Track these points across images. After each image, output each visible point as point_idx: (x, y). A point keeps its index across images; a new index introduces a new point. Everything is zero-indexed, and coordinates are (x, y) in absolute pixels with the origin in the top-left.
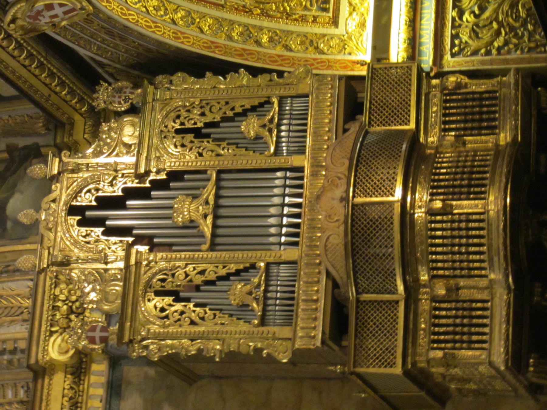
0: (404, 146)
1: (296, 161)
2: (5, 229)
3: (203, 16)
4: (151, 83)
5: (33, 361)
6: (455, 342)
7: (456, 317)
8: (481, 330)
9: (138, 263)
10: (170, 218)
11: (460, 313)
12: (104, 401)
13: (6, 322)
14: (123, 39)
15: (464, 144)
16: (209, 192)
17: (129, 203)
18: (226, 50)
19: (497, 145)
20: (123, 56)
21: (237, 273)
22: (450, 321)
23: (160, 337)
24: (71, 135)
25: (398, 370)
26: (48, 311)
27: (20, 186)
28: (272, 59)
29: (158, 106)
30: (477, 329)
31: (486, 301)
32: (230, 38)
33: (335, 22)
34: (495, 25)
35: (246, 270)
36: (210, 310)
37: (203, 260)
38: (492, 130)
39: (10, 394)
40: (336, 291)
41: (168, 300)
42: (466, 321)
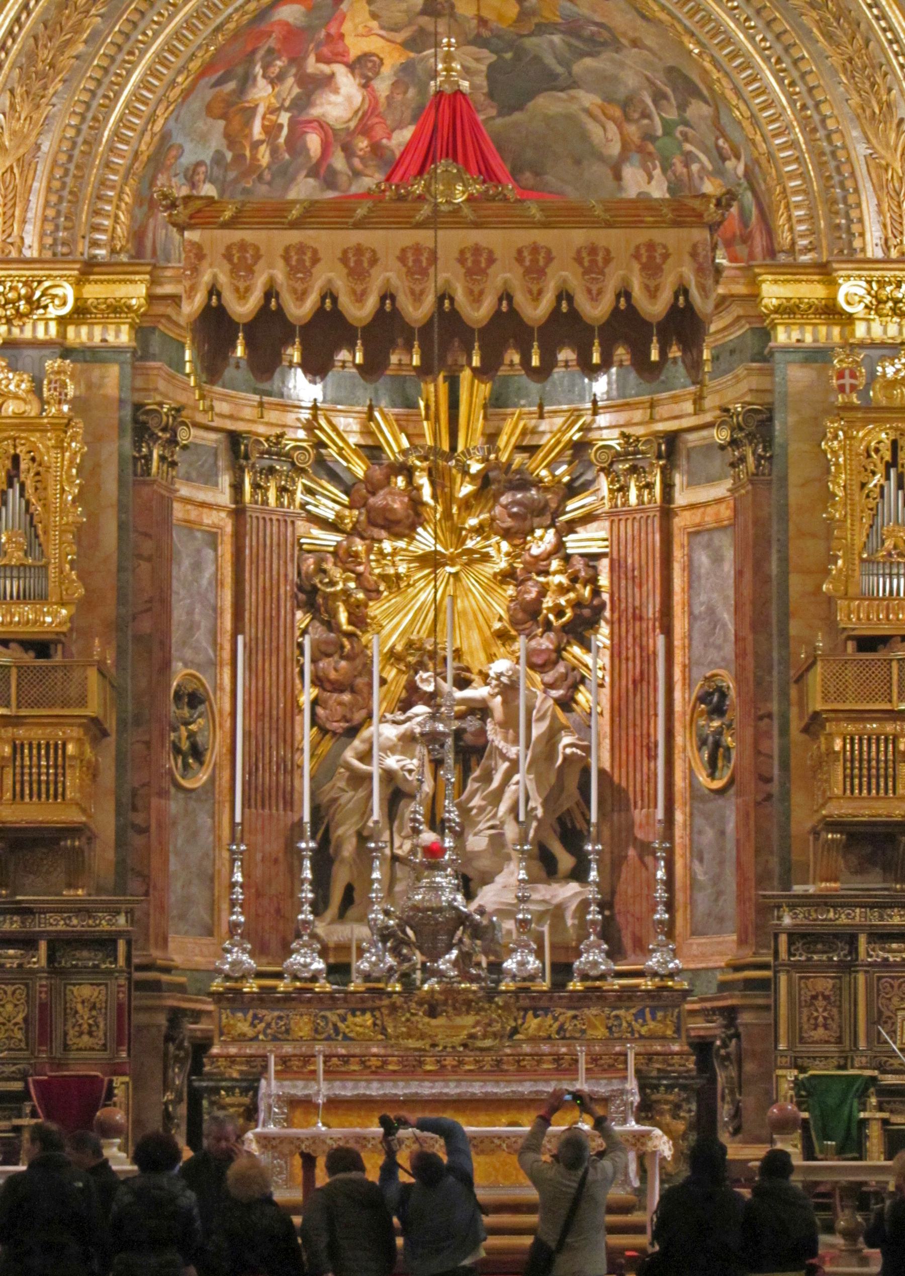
5: (835, 266)
6: (852, 761)
7: (878, 761)
8: (865, 787)
11: (882, 765)
12: (799, 345)
13: (885, 218)
22: (873, 754)
25: (819, 707)
26: (895, 277)
30: (865, 784)
31: (894, 792)
36: (877, 504)
39: (803, 227)
40: (899, 639)
41: (888, 457)
42: (874, 771)
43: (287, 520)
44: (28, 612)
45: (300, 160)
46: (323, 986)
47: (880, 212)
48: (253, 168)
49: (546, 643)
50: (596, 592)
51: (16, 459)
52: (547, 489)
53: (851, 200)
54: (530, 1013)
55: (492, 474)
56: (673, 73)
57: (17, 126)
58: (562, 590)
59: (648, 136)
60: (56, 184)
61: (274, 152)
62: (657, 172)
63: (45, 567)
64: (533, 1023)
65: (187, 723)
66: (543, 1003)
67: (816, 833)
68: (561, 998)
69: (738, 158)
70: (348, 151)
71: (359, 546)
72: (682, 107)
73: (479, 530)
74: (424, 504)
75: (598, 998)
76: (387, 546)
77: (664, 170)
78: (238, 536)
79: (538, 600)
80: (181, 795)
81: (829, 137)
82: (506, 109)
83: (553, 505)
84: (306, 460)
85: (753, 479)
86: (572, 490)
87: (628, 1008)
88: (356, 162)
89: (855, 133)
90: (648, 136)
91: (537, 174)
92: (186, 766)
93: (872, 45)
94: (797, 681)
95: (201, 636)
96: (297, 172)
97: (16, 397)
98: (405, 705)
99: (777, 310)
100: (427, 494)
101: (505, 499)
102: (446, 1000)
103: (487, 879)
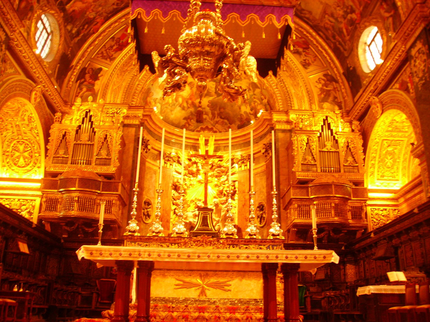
0: (347, 197)
1: (342, 171)
2: (321, 102)
3: (378, 146)
4: (360, 134)
9: (314, 134)
10: (327, 141)
14: (371, 126)
15: (349, 212)
16: (333, 150)
17: (330, 131)
18: (369, 152)
19: (349, 219)
20: (366, 127)
21: (314, 158)
23: (297, 140)
24: (346, 116)
25: (292, 197)
27: (332, 105)
28: (367, 164)
29: (354, 136)
32: (372, 153)
33: (378, 179)
34: (379, 219)
35: (315, 160)
37: (316, 149)
38: (352, 218)
39: (281, 106)
41: (306, 141)
44: (105, 167)
45: (177, 103)
47: (297, 103)
48: (168, 103)
49: (224, 198)
50: (235, 188)
51: (106, 135)
52: (225, 168)
53: (292, 100)
54: (231, 246)
55: (214, 164)
57: (118, 80)
58: (228, 187)
60: (125, 91)
61: (172, 100)
62: (248, 107)
63: (110, 159)
65: (147, 209)
66: (236, 243)
68: (242, 241)
69: (265, 99)
70: (187, 102)
72: (254, 91)
73: (210, 176)
74: (199, 170)
75: (255, 242)
76: (192, 178)
77: (250, 105)
79: (223, 190)
80: (144, 224)
81: (286, 89)
83: (226, 171)
87: (264, 245)
88: (189, 105)
89: (291, 88)
91: (224, 109)
92: (146, 218)
93: (295, 72)
94: (282, 198)
96: (177, 105)
97: (108, 122)
99: (277, 121)
100: (200, 168)
101: (216, 170)
102: (203, 240)
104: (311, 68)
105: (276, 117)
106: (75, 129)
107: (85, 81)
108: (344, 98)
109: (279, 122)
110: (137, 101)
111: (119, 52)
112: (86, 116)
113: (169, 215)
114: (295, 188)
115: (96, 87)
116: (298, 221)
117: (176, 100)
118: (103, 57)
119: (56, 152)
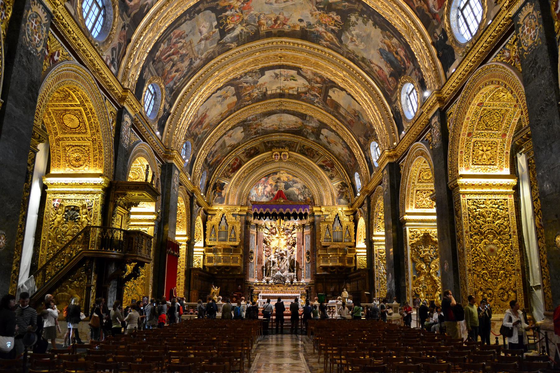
38: (348, 263)
43: (262, 233)
46: (266, 284)
48: (259, 196)
49: (290, 247)
56: (304, 186)
59: (301, 193)
64: (289, 288)
67: (319, 267)
70: (269, 194)
71: (270, 236)
76: (273, 236)
78: (257, 235)
82: (286, 190)
84: (264, 227)
85: (312, 229)
86: (293, 230)
90: (301, 193)
95: (253, 246)
98: (275, 253)
100: (277, 230)
103: (283, 272)
104: (334, 179)
105: (315, 209)
106: (218, 224)
107: (217, 190)
108: (351, 196)
109: (316, 211)
110: (244, 201)
111: (233, 174)
112: (223, 217)
113: (262, 257)
114: (321, 249)
115: (223, 194)
116: (321, 265)
117: (263, 193)
118: (225, 176)
119: (211, 236)
